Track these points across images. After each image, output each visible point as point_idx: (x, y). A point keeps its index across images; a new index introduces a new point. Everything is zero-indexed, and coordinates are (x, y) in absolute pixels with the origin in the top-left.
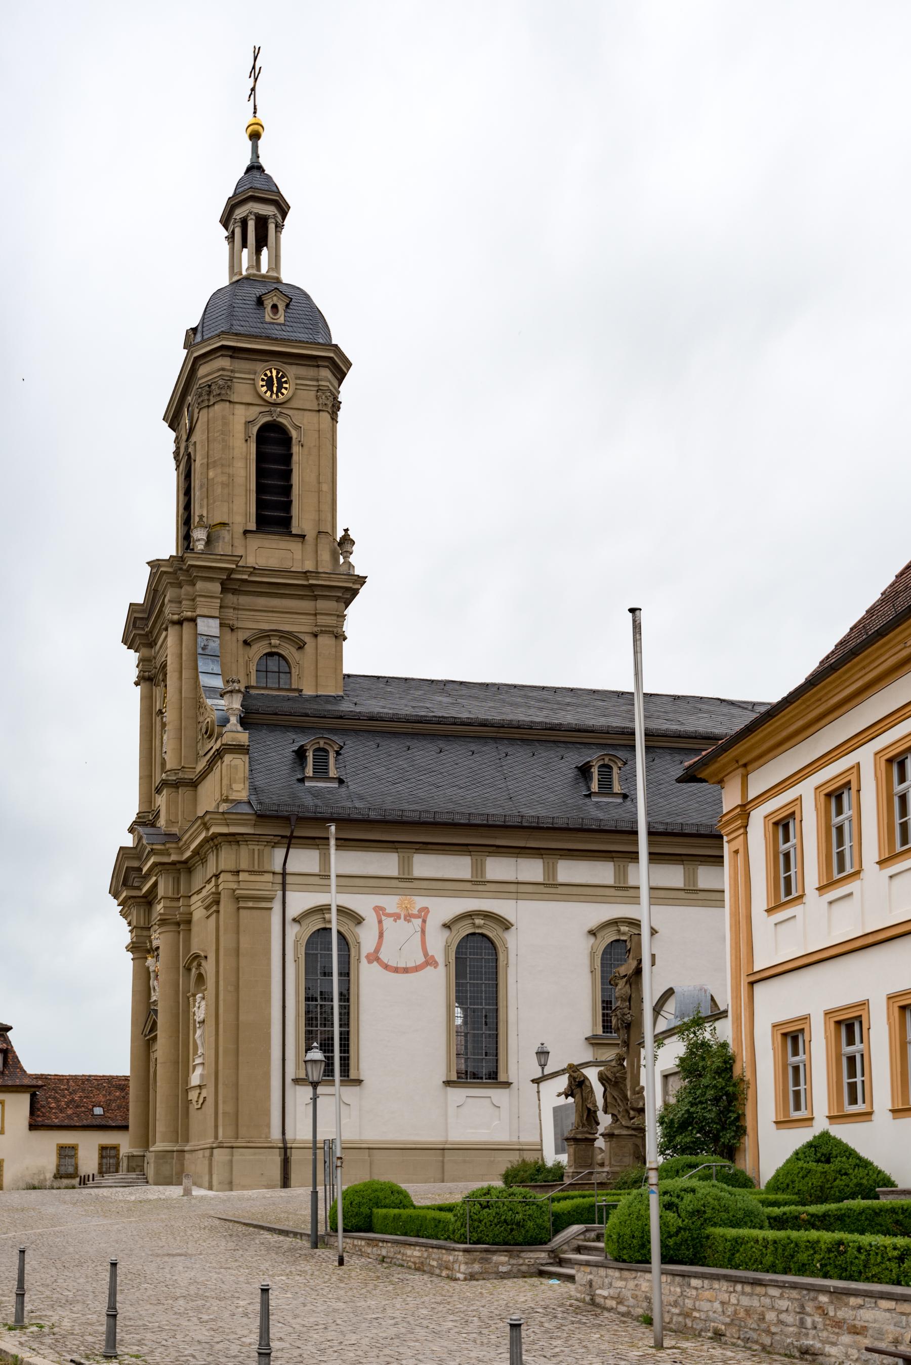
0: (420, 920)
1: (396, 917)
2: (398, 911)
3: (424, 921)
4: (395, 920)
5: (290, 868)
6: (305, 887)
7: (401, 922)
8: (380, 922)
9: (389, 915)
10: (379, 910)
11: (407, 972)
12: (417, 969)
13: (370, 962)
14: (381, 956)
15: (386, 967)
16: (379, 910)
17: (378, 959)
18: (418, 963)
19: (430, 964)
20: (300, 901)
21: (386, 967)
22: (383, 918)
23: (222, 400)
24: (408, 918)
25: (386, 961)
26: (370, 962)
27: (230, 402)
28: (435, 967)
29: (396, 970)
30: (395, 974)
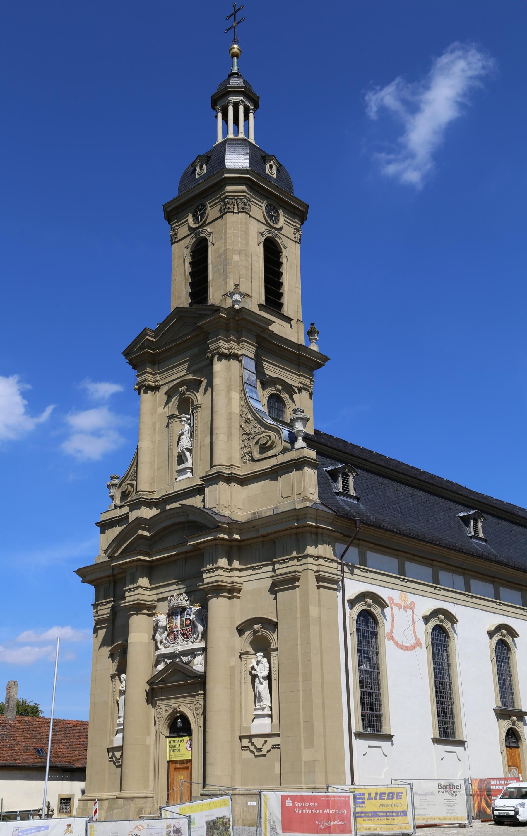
2: (399, 602)
3: (413, 612)
4: (399, 609)
8: (392, 609)
9: (396, 605)
11: (408, 650)
12: (413, 647)
13: (389, 640)
15: (397, 644)
17: (392, 638)
21: (397, 644)
22: (393, 606)
24: (406, 608)
25: (396, 640)
26: (389, 640)
27: (250, 216)
30: (402, 651)
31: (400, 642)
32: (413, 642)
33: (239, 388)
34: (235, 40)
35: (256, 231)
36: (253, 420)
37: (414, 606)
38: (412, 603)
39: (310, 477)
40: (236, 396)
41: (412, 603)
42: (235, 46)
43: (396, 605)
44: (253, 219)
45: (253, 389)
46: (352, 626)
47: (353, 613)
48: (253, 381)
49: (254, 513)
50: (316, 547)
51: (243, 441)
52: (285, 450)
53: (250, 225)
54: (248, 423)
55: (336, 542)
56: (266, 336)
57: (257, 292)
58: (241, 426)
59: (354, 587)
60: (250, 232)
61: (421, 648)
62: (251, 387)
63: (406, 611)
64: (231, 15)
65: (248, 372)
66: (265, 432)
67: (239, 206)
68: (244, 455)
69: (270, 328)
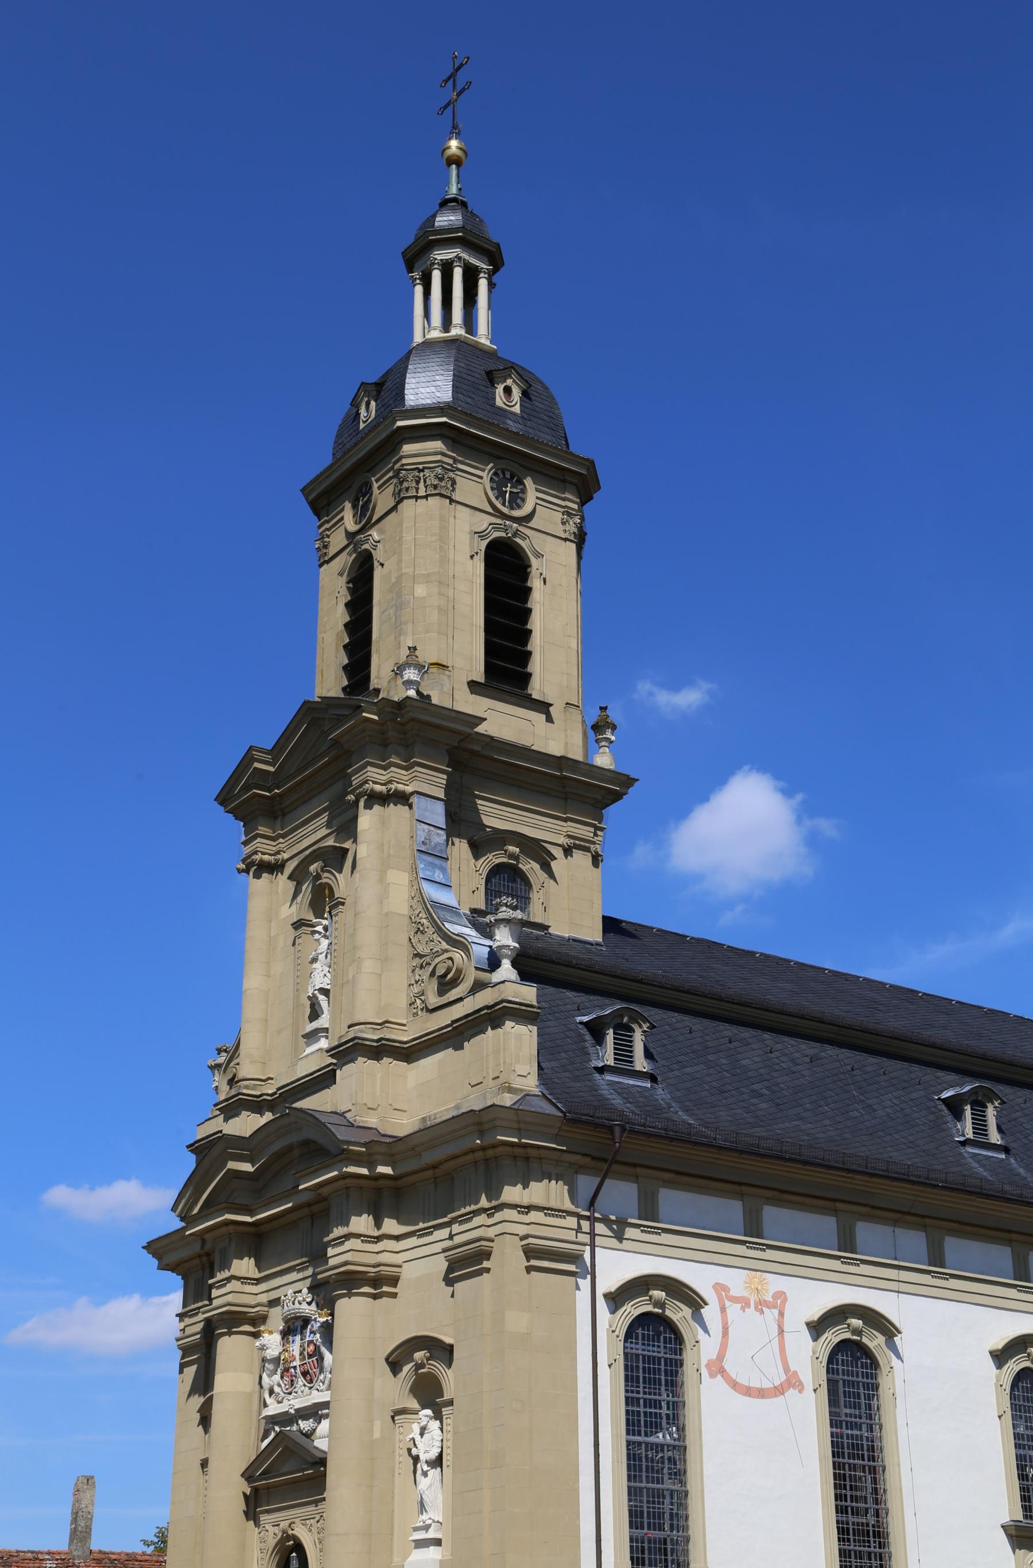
0: (776, 1312)
1: (745, 1303)
2: (746, 1294)
3: (781, 1314)
4: (743, 1309)
7: (751, 1311)
8: (723, 1310)
9: (735, 1300)
10: (720, 1288)
11: (763, 1397)
13: (712, 1375)
14: (727, 1365)
15: (735, 1385)
16: (720, 1288)
17: (722, 1371)
18: (777, 1383)
19: (794, 1386)
21: (735, 1385)
22: (727, 1303)
23: (441, 495)
24: (761, 1306)
25: (734, 1376)
26: (712, 1375)
27: (452, 501)
28: (800, 1391)
29: (748, 1392)
30: (747, 1398)
31: (743, 1380)
32: (778, 1378)
34: (455, 131)
35: (467, 529)
37: (785, 1300)
38: (781, 1295)
39: (519, 1041)
41: (781, 1295)
42: (454, 144)
43: (735, 1300)
44: (459, 507)
46: (611, 1349)
47: (612, 1324)
48: (437, 844)
49: (424, 1119)
50: (525, 1186)
52: (479, 986)
53: (452, 519)
55: (576, 1172)
56: (477, 748)
57: (469, 654)
59: (617, 1265)
60: (451, 534)
61: (800, 1391)
63: (762, 1312)
64: (447, 81)
66: (447, 951)
67: (428, 482)
69: (481, 729)
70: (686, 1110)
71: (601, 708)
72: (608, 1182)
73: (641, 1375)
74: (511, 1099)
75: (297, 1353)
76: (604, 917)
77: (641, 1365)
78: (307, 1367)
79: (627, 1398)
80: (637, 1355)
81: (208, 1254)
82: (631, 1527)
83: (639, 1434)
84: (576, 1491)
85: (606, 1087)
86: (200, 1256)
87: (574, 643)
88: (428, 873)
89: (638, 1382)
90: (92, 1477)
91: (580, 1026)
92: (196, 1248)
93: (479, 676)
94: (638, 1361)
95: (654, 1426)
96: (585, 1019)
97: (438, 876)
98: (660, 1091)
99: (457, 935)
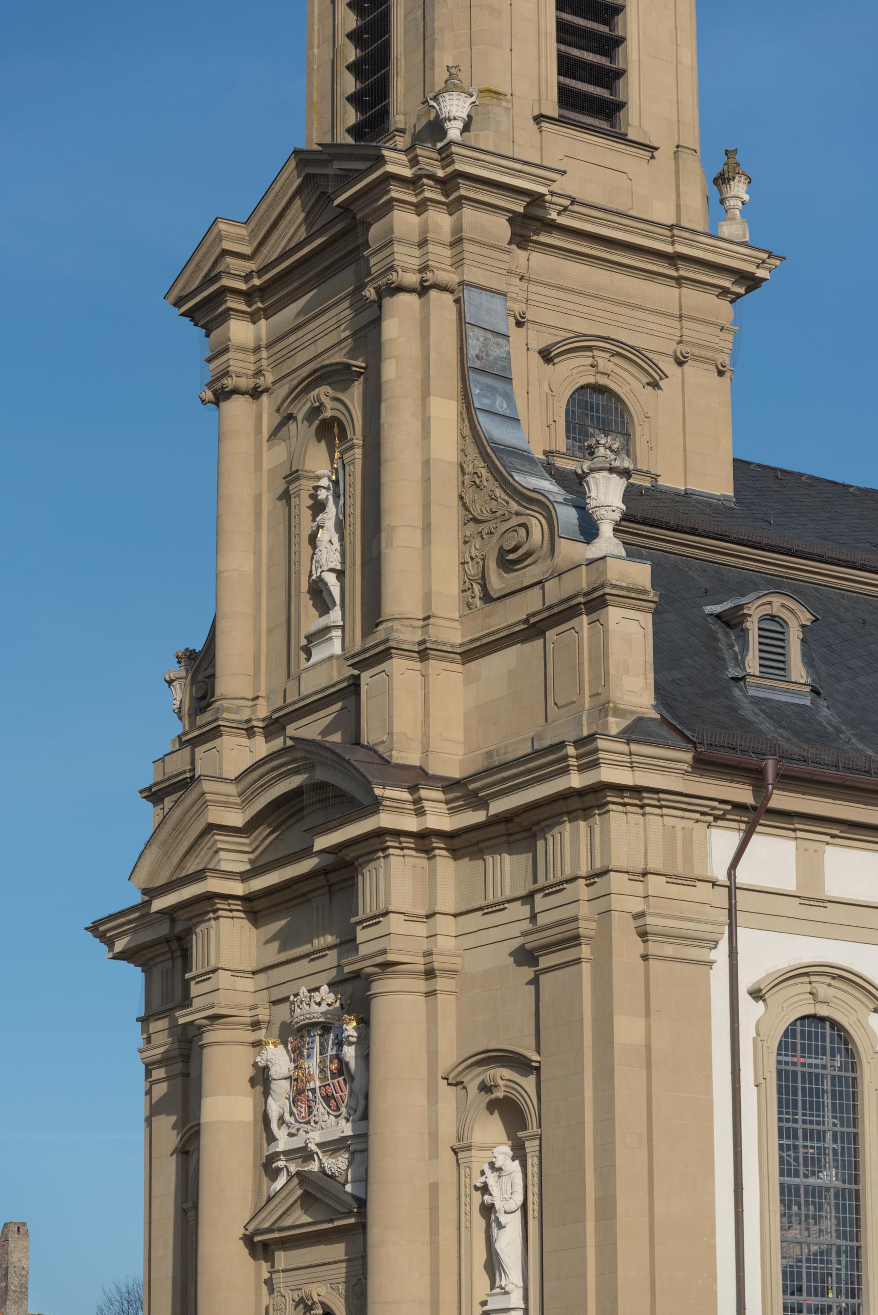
5: (743, 877)
6: (773, 922)
20: (766, 952)
33: (453, 384)
36: (491, 478)
40: (445, 411)
45: (498, 384)
51: (466, 542)
54: (478, 487)
58: (461, 498)
62: (489, 381)
65: (481, 333)
68: (468, 584)
70: (862, 738)
71: (727, 152)
72: (755, 838)
73: (800, 1098)
74: (617, 724)
75: (315, 1071)
76: (735, 460)
77: (799, 1085)
78: (330, 1090)
79: (780, 1129)
80: (795, 1073)
81: (179, 939)
82: (785, 1292)
83: (797, 1175)
84: (712, 1248)
85: (749, 706)
86: (168, 941)
87: (688, 56)
88: (486, 401)
89: (795, 1107)
90: (24, 1224)
91: (709, 620)
92: (163, 929)
93: (552, 109)
94: (795, 1080)
95: (815, 1164)
96: (718, 609)
97: (500, 405)
98: (825, 712)
99: (534, 491)
